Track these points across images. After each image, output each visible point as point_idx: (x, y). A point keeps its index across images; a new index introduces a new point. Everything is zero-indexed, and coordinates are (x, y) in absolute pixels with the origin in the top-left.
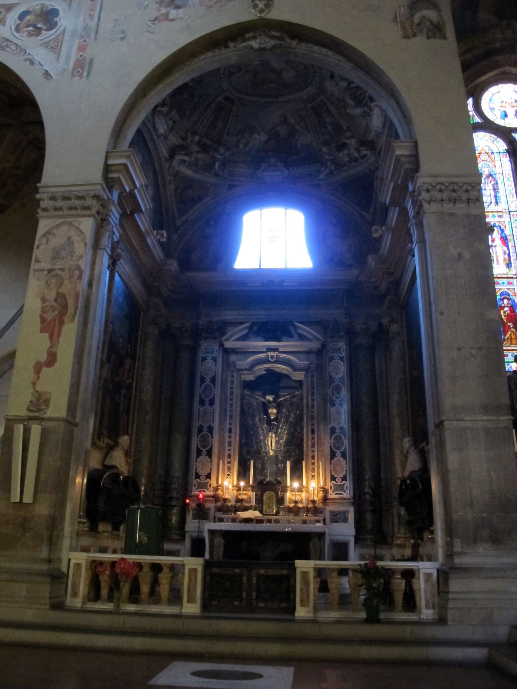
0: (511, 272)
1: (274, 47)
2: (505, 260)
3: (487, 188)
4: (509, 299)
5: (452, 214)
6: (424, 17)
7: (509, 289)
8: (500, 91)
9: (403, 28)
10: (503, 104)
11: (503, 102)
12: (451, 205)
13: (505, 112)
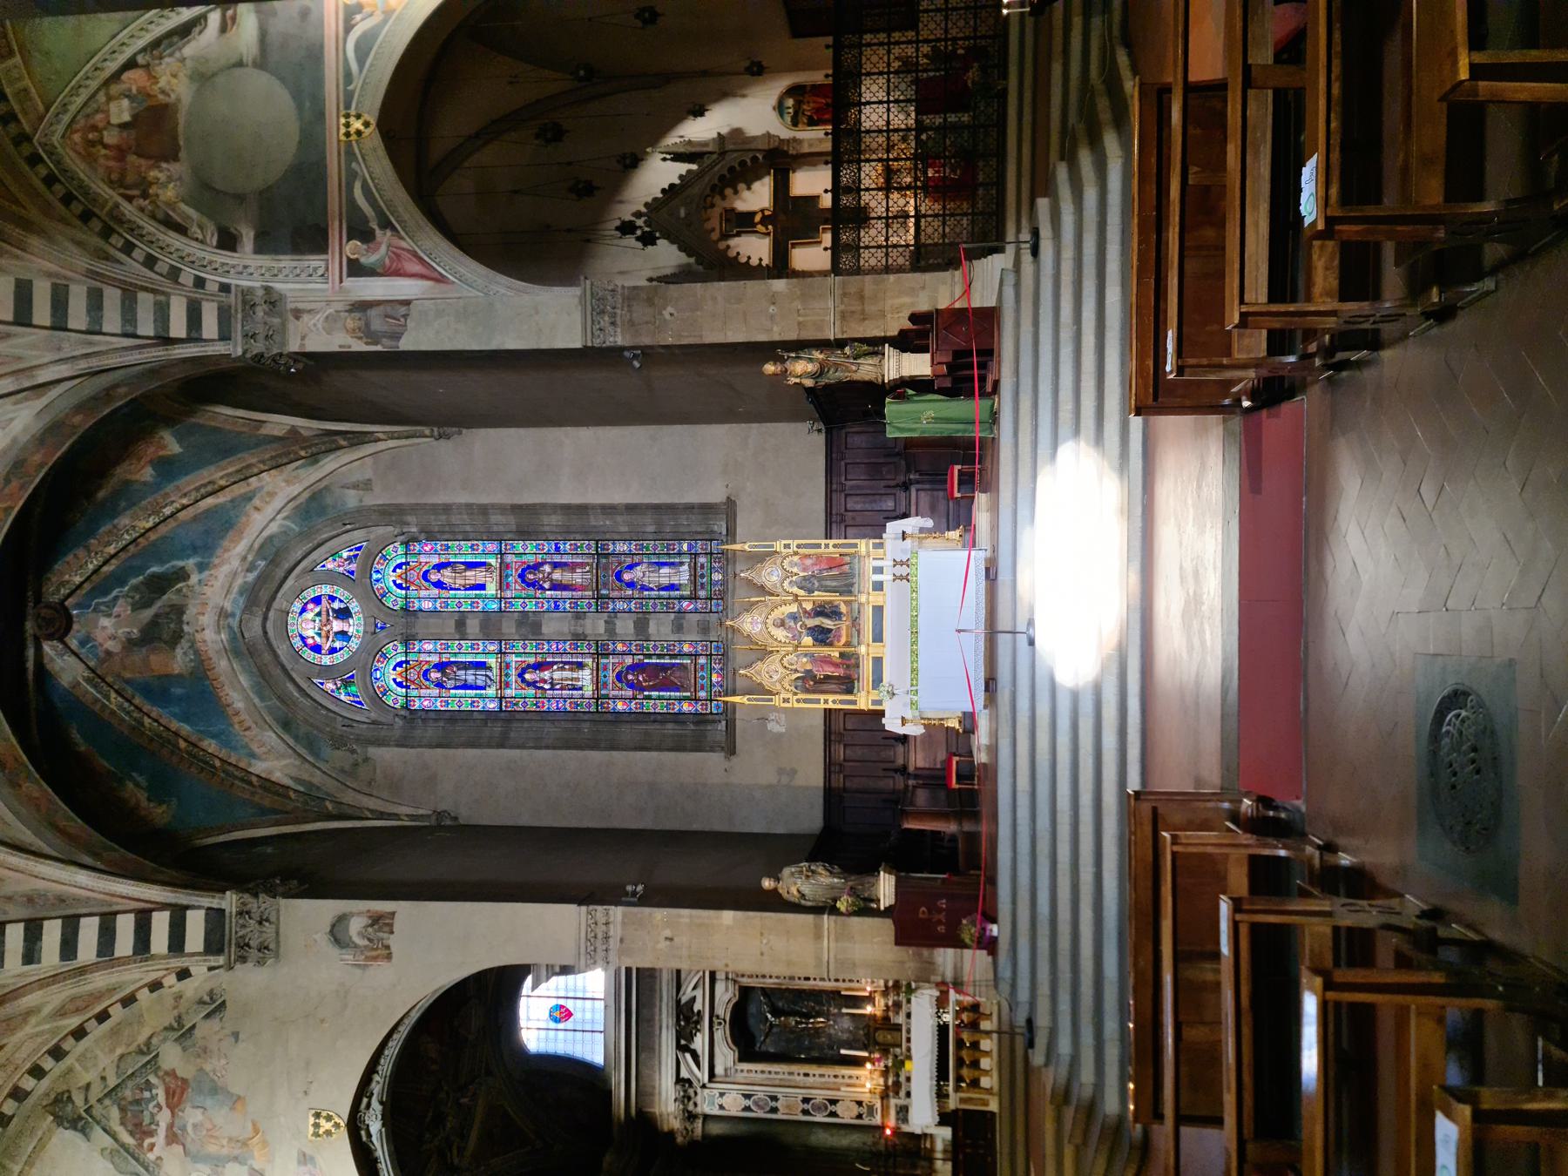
0: (590, 664)
1: (381, 1103)
2: (571, 670)
4: (627, 673)
5: (622, 940)
6: (360, 934)
7: (613, 671)
8: (301, 636)
9: (375, 958)
10: (323, 634)
11: (319, 635)
12: (611, 940)
13: (337, 633)
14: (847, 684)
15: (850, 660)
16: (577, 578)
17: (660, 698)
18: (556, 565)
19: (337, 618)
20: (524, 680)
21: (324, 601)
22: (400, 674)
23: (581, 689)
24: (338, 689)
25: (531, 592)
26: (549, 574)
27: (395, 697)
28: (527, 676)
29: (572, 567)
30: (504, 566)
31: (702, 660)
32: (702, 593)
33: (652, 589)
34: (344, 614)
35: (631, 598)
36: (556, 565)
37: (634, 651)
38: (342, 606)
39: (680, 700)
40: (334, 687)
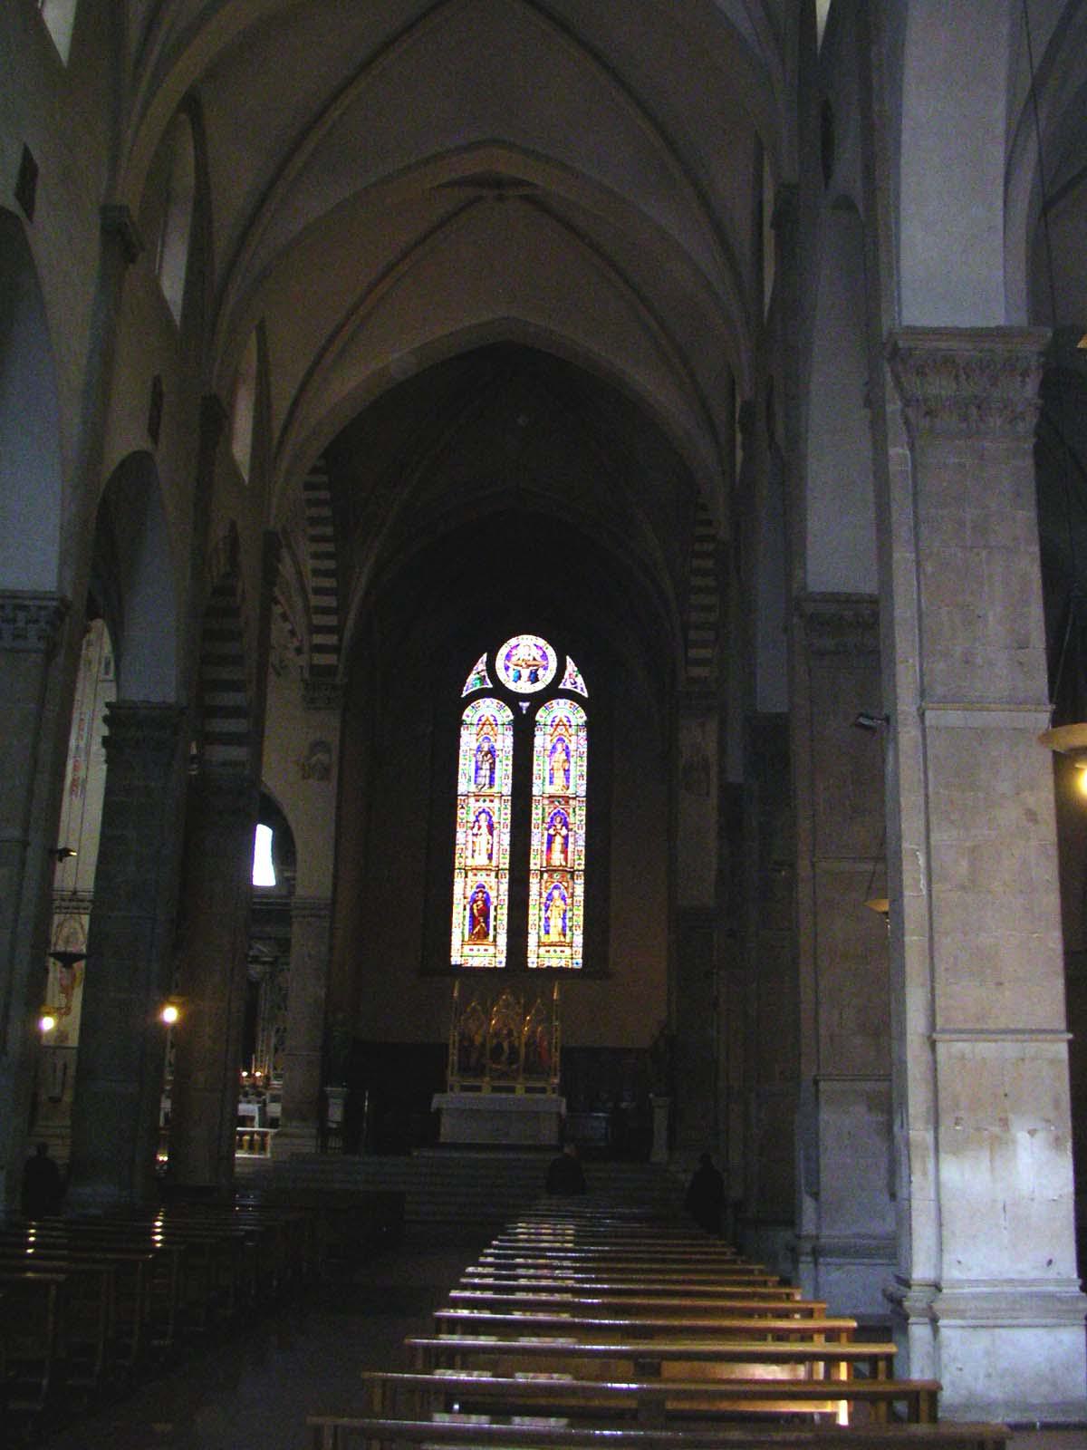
3: (484, 767)
8: (518, 645)
13: (519, 671)
14: (465, 1069)
15: (479, 1071)
16: (557, 859)
17: (464, 917)
18: (566, 838)
19: (531, 672)
20: (480, 813)
21: (545, 663)
22: (487, 720)
23: (473, 857)
24: (478, 673)
25: (548, 820)
26: (560, 834)
27: (469, 715)
28: (483, 816)
29: (565, 851)
30: (567, 799)
31: (491, 949)
32: (543, 950)
33: (546, 911)
34: (534, 678)
35: (540, 895)
36: (566, 838)
37: (500, 898)
38: (540, 677)
39: (463, 933)
40: (479, 670)
